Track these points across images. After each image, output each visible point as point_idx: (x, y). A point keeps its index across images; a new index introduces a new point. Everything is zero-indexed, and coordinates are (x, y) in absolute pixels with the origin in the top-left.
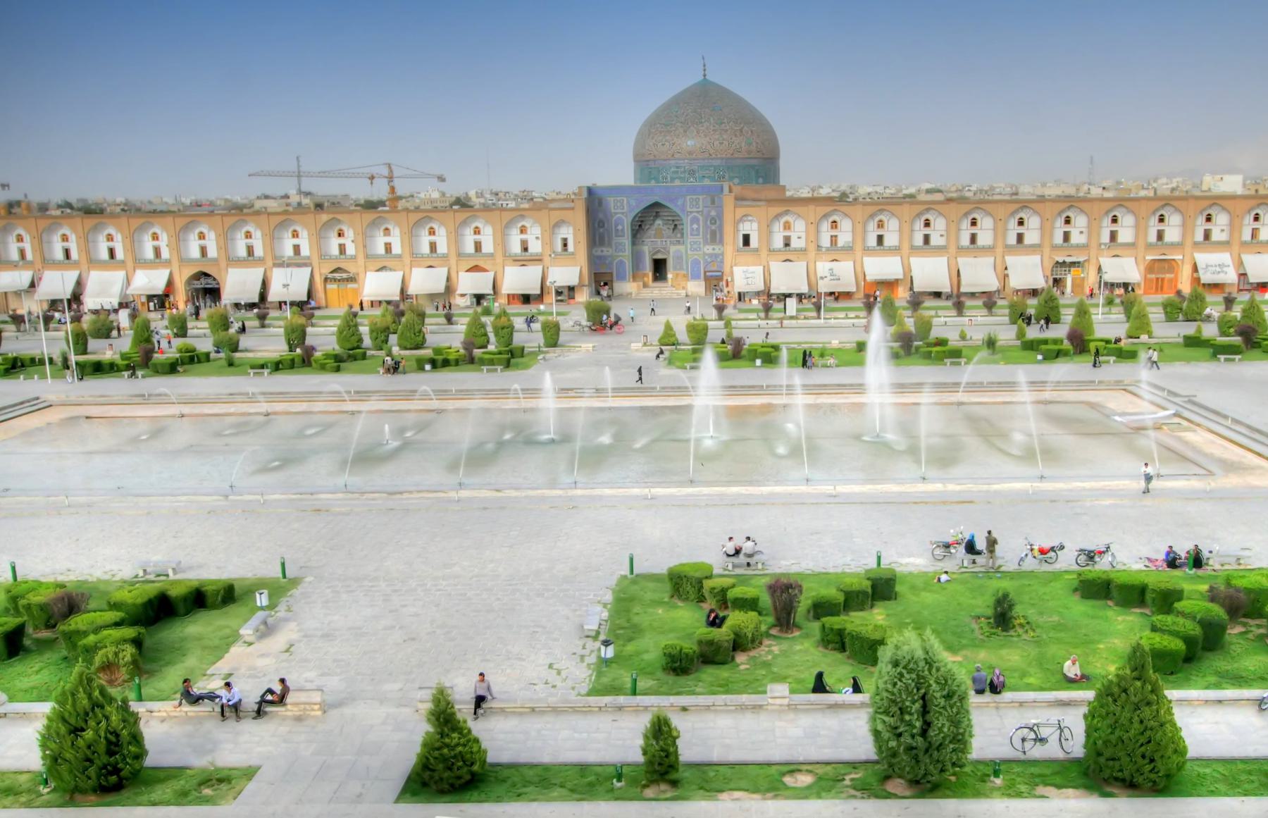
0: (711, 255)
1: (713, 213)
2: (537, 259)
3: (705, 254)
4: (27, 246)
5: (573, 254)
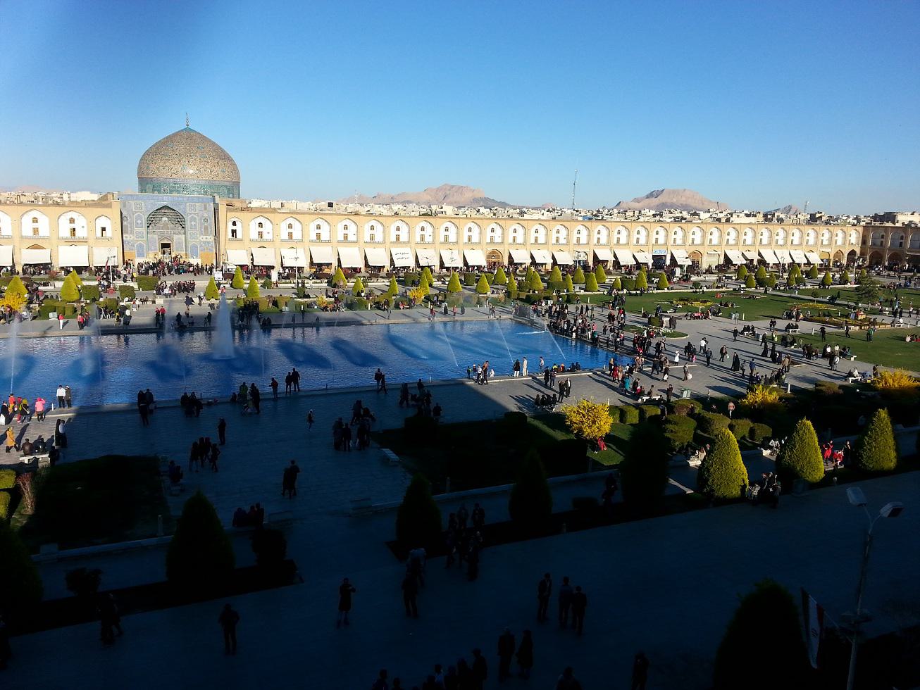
0: (205, 242)
1: (206, 215)
2: (84, 241)
3: (200, 241)
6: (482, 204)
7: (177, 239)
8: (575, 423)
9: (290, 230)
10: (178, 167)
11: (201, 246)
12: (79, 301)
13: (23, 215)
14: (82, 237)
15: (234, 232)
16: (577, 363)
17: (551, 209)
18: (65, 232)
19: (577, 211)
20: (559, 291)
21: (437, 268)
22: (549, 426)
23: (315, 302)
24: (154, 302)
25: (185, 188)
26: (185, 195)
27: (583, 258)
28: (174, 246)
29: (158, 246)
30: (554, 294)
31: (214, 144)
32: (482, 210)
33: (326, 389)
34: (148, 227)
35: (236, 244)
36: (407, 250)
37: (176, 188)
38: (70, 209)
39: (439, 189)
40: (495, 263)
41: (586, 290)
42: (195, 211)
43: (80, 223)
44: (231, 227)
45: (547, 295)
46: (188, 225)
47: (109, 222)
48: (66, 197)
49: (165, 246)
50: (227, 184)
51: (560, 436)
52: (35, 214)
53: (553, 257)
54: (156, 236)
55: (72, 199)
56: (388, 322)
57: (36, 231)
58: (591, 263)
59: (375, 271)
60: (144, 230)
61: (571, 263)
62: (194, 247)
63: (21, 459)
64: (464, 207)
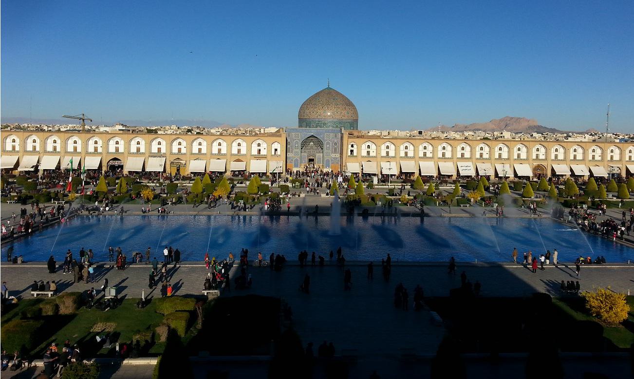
0: (334, 158)
1: (336, 141)
2: (264, 157)
4: (17, 144)
5: (356, 156)
6: (535, 130)
7: (319, 155)
8: (594, 307)
9: (388, 150)
10: (321, 111)
11: (332, 160)
12: (256, 194)
13: (233, 142)
14: (262, 155)
15: (352, 151)
16: (602, 257)
17: (593, 134)
18: (254, 152)
19: (616, 135)
20: (593, 198)
21: (492, 177)
22: (572, 308)
23: (399, 200)
24: (299, 196)
25: (325, 124)
26: (325, 128)
27: (616, 171)
28: (316, 160)
29: (307, 160)
30: (590, 200)
31: (343, 96)
32: (535, 134)
33: (397, 262)
34: (302, 148)
35: (352, 159)
36: (470, 164)
37: (320, 124)
38: (258, 138)
39: (501, 120)
40: (540, 174)
41: (618, 197)
42: (329, 138)
43: (264, 146)
44: (350, 148)
45: (583, 200)
46: (325, 147)
47: (279, 146)
48: (262, 131)
49: (311, 160)
50: (349, 121)
51: (579, 316)
52: (239, 141)
53: (590, 171)
54: (306, 154)
55: (266, 132)
56: (450, 215)
57: (239, 151)
58: (624, 175)
59: (442, 178)
60: (299, 151)
61: (606, 176)
62: (328, 161)
63: (203, 292)
64: (521, 133)
